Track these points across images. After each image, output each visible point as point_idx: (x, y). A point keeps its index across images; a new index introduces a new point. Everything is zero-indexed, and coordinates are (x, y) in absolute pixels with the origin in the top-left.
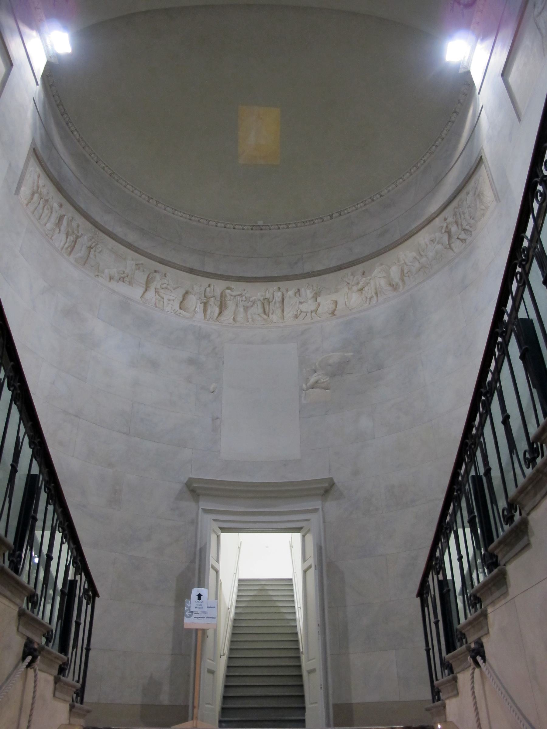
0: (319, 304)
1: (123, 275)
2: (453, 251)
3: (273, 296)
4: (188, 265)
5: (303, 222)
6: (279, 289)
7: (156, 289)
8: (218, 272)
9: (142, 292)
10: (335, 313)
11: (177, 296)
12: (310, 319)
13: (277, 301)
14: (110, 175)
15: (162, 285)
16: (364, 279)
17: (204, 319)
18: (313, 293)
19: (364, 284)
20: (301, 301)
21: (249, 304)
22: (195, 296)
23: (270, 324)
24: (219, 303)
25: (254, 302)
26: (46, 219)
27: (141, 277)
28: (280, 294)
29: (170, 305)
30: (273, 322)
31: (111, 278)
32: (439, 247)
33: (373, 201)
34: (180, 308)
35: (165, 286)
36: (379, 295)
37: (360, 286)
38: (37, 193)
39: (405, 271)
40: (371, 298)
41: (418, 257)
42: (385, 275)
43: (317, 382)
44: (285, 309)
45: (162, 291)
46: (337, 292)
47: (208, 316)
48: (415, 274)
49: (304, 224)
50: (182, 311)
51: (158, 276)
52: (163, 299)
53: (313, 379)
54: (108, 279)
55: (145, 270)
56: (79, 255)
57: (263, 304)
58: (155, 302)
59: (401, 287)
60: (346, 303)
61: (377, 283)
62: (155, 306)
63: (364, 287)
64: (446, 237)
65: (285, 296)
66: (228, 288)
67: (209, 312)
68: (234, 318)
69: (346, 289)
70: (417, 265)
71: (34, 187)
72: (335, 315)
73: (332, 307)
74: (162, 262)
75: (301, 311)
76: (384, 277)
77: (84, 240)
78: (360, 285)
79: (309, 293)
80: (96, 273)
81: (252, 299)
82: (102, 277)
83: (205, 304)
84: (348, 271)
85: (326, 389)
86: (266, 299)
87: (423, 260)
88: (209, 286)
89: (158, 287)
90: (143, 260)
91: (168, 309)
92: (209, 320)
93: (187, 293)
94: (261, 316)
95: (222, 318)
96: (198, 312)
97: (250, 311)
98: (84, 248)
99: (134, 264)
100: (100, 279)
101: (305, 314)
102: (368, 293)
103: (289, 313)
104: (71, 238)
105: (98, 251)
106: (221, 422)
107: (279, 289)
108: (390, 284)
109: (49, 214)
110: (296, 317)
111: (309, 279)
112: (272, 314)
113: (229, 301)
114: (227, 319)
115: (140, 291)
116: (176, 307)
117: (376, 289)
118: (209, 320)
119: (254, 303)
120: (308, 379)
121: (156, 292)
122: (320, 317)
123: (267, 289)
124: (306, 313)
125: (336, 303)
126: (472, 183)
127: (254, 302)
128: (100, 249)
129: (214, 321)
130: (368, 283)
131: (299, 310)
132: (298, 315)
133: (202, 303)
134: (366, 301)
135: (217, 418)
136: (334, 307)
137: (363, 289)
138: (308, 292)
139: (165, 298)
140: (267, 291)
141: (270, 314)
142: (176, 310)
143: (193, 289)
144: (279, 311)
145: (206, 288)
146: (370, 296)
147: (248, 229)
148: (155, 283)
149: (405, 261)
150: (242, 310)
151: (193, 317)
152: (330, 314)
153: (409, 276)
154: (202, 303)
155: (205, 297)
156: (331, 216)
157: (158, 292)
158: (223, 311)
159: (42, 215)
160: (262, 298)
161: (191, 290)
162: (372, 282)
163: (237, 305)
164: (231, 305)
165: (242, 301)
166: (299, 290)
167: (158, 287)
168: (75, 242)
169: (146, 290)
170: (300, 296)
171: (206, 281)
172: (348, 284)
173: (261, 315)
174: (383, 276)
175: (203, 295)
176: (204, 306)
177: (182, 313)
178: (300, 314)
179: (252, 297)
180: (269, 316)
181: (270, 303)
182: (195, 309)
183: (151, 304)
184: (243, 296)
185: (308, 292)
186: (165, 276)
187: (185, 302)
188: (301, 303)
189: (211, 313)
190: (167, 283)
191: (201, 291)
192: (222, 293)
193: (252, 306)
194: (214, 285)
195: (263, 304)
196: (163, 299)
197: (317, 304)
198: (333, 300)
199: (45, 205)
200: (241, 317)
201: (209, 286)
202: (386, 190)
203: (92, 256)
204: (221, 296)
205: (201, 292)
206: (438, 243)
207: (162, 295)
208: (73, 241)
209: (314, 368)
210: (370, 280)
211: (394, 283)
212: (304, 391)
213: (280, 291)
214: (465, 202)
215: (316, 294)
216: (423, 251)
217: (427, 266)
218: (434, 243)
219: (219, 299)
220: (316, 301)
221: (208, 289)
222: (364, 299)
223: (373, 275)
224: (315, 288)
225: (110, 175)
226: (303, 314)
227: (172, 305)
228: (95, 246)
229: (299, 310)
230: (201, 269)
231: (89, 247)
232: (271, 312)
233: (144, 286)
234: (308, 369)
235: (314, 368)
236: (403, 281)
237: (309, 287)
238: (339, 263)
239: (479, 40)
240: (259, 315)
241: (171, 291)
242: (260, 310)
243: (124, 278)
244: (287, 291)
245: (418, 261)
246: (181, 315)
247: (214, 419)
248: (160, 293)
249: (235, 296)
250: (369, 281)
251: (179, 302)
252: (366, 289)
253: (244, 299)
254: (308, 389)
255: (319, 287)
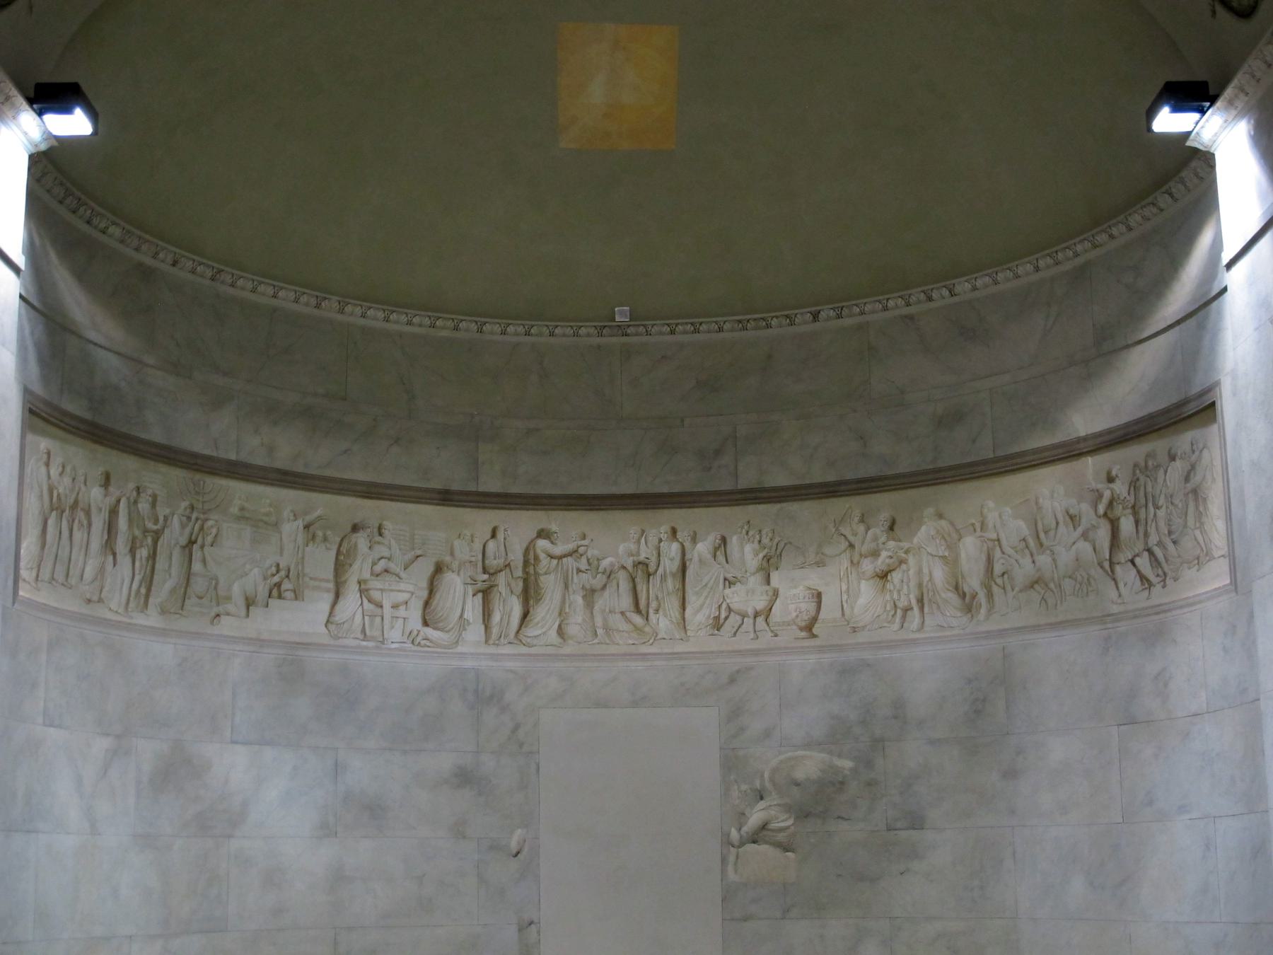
0: (776, 593)
1: (276, 579)
2: (1117, 588)
3: (659, 555)
4: (436, 484)
5: (740, 321)
6: (674, 531)
7: (359, 583)
8: (514, 490)
9: (325, 607)
10: (815, 631)
11: (411, 587)
12: (752, 635)
13: (668, 571)
14: (213, 279)
15: (374, 564)
16: (892, 544)
17: (486, 642)
18: (761, 556)
19: (892, 560)
20: (729, 576)
21: (598, 581)
22: (459, 574)
23: (651, 641)
24: (519, 586)
25: (608, 572)
26: (81, 558)
27: (321, 560)
28: (675, 547)
29: (401, 621)
30: (658, 637)
31: (249, 603)
32: (1084, 547)
33: (930, 299)
34: (426, 623)
35: (382, 564)
36: (926, 610)
37: (882, 561)
38: (52, 510)
39: (998, 569)
40: (907, 610)
41: (1032, 543)
42: (947, 554)
43: (764, 827)
44: (690, 597)
45: (375, 584)
46: (820, 564)
47: (495, 631)
48: (1021, 591)
49: (740, 325)
50: (429, 632)
51: (361, 540)
52: (382, 607)
53: (755, 818)
54: (243, 612)
55: (329, 533)
56: (169, 585)
57: (633, 580)
58: (362, 624)
59: (983, 611)
60: (842, 606)
61: (926, 571)
62: (361, 637)
63: (890, 571)
64: (1103, 534)
65: (687, 557)
66: (543, 534)
67: (496, 617)
68: (560, 626)
69: (846, 563)
70: (1024, 569)
71: (42, 492)
72: (814, 636)
73: (808, 607)
74: (372, 491)
75: (730, 610)
76: (943, 557)
77: (175, 534)
78: (880, 560)
79: (747, 554)
80: (215, 610)
81: (605, 563)
82: (228, 614)
83: (486, 593)
84: (853, 505)
85: (786, 849)
86: (640, 563)
87: (1044, 560)
88: (494, 535)
89: (366, 575)
90: (322, 504)
91: (394, 634)
92: (497, 642)
93: (439, 569)
94: (628, 621)
95: (530, 631)
96: (469, 623)
97: (601, 603)
98: (177, 554)
99: (301, 527)
100: (227, 626)
101: (739, 618)
102: (899, 591)
103: (699, 614)
104: (143, 553)
105: (209, 539)
106: (539, 932)
107: (674, 531)
108: (957, 588)
109: (86, 535)
110: (717, 624)
111: (751, 508)
112: (657, 611)
113: (546, 574)
114: (544, 633)
115: (324, 606)
116: (415, 622)
117: (920, 586)
118: (497, 642)
119: (609, 577)
120: (744, 814)
121: (360, 591)
122: (776, 636)
123: (643, 531)
124: (742, 616)
125: (819, 595)
126: (1201, 314)
127: (609, 575)
128: (214, 531)
129: (510, 643)
130: (901, 562)
131: (724, 606)
132: (722, 621)
133: (480, 591)
134: (893, 616)
135: (530, 924)
136: (813, 613)
137: (889, 578)
138: (748, 548)
139: (384, 606)
140: (643, 540)
141: (651, 611)
142: (415, 632)
143: (452, 554)
144: (672, 604)
145: (487, 541)
146: (903, 603)
147: (588, 335)
148: (356, 566)
149: (998, 535)
150: (579, 600)
151: (457, 642)
152: (801, 629)
153: (1004, 588)
154: (480, 591)
155: (485, 571)
156: (815, 316)
157: (367, 590)
158: (531, 610)
159: (70, 560)
160: (629, 563)
161: (448, 559)
162: (911, 560)
163: (566, 587)
164: (550, 584)
165: (579, 571)
166: (724, 540)
167: (366, 575)
168: (153, 556)
169: (337, 596)
170: (727, 562)
171: (480, 520)
172: (851, 546)
173: (628, 614)
174: (941, 554)
175: (480, 569)
176: (483, 598)
177: (430, 637)
178: (726, 618)
179: (604, 558)
180: (647, 619)
181: (651, 577)
182: (461, 616)
183: (352, 636)
184: (581, 555)
185: (748, 548)
186: (380, 534)
187: (434, 603)
188: (729, 582)
189: (501, 619)
190: (386, 554)
191: (473, 554)
192: (527, 551)
193: (604, 587)
194: (505, 530)
195: (633, 580)
196: (379, 610)
197: (771, 593)
198: (810, 589)
199: (73, 521)
200: (577, 618)
201: (494, 535)
202: (966, 284)
203: (197, 566)
204: (526, 563)
205: (473, 559)
206: (1085, 536)
207: (376, 595)
208: (148, 560)
209: (758, 784)
210: (907, 552)
211: (966, 589)
212: (733, 847)
213: (678, 540)
214: (1161, 472)
215: (768, 559)
216: (1046, 532)
217: (1052, 585)
218: (1075, 528)
219: (519, 573)
220: (768, 583)
221: (491, 545)
222: (888, 608)
223: (915, 540)
224: (766, 541)
225: (213, 279)
226: (734, 620)
227: (404, 619)
228: (202, 528)
229: (724, 606)
230: (472, 488)
231: (184, 547)
232: (654, 605)
233: (331, 585)
234: (744, 787)
235: (759, 787)
236: (990, 595)
237: (751, 533)
238: (831, 477)
239: (1248, 115)
240: (622, 613)
241: (398, 575)
242: (626, 602)
243: (278, 585)
244: (694, 540)
245: (1032, 555)
246: (428, 644)
247: (525, 926)
248: (372, 593)
249: (560, 558)
250: (903, 555)
251: (420, 604)
252: (896, 577)
253: (583, 564)
254: (742, 844)
255: (776, 541)
